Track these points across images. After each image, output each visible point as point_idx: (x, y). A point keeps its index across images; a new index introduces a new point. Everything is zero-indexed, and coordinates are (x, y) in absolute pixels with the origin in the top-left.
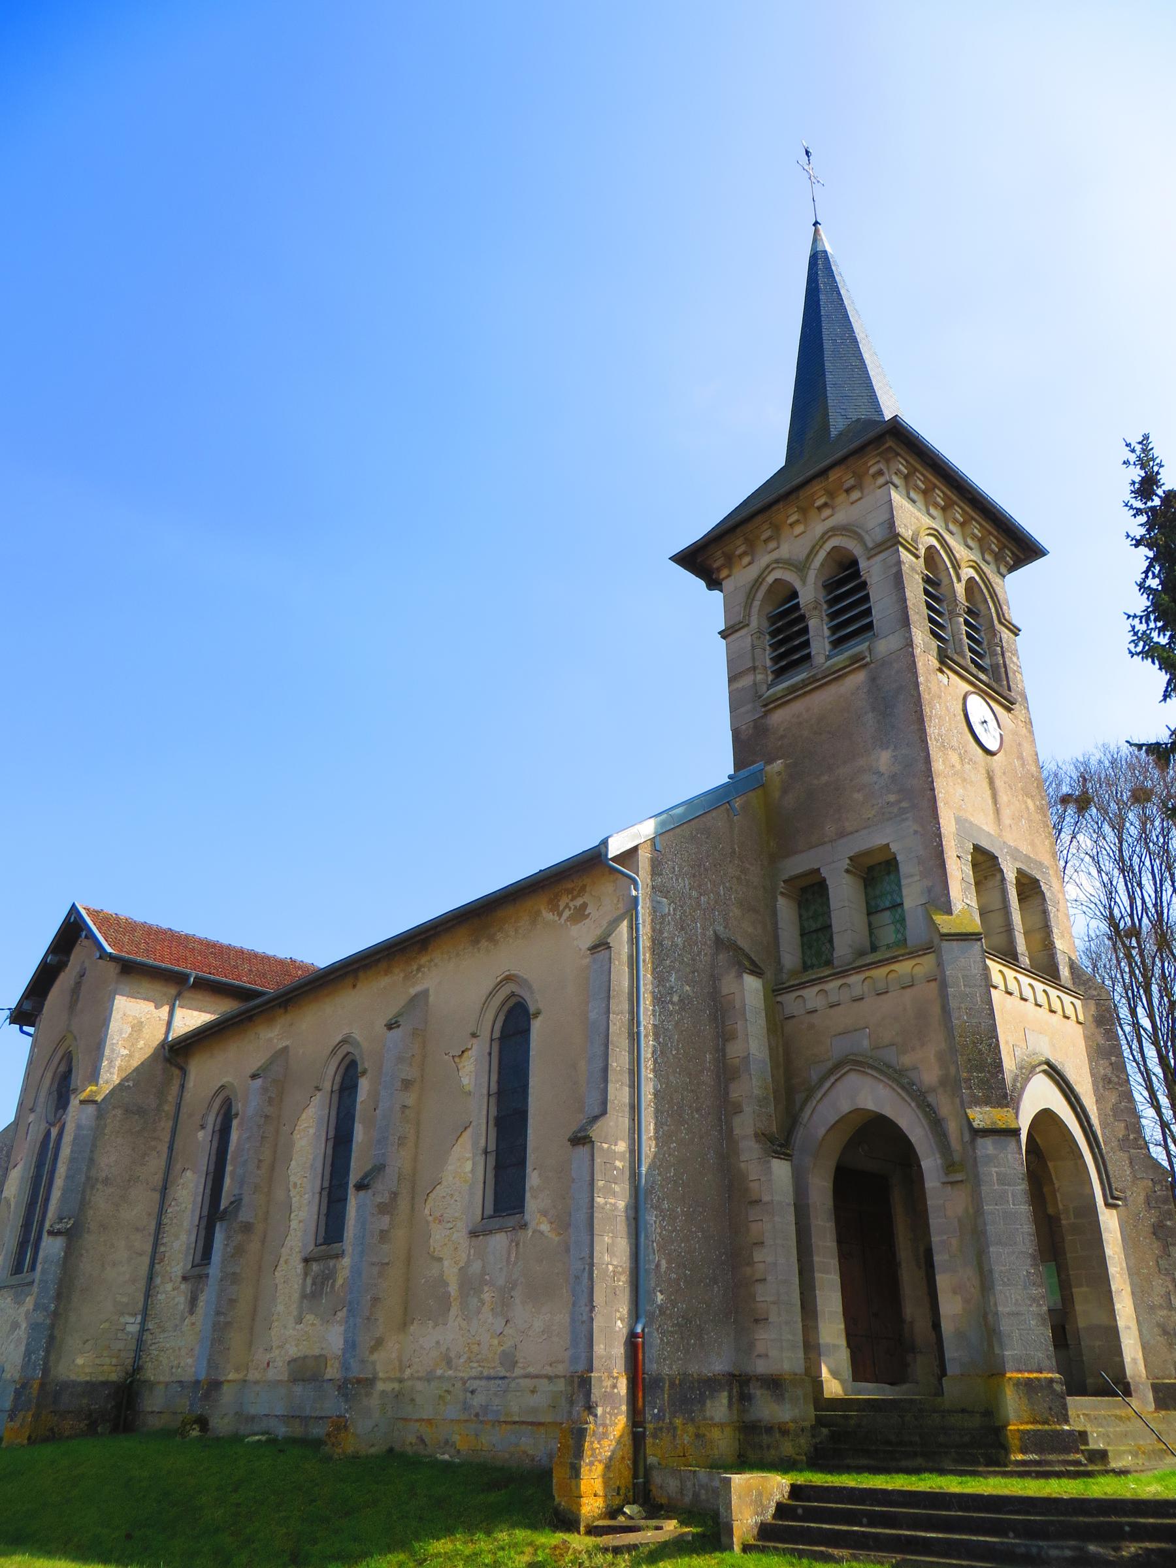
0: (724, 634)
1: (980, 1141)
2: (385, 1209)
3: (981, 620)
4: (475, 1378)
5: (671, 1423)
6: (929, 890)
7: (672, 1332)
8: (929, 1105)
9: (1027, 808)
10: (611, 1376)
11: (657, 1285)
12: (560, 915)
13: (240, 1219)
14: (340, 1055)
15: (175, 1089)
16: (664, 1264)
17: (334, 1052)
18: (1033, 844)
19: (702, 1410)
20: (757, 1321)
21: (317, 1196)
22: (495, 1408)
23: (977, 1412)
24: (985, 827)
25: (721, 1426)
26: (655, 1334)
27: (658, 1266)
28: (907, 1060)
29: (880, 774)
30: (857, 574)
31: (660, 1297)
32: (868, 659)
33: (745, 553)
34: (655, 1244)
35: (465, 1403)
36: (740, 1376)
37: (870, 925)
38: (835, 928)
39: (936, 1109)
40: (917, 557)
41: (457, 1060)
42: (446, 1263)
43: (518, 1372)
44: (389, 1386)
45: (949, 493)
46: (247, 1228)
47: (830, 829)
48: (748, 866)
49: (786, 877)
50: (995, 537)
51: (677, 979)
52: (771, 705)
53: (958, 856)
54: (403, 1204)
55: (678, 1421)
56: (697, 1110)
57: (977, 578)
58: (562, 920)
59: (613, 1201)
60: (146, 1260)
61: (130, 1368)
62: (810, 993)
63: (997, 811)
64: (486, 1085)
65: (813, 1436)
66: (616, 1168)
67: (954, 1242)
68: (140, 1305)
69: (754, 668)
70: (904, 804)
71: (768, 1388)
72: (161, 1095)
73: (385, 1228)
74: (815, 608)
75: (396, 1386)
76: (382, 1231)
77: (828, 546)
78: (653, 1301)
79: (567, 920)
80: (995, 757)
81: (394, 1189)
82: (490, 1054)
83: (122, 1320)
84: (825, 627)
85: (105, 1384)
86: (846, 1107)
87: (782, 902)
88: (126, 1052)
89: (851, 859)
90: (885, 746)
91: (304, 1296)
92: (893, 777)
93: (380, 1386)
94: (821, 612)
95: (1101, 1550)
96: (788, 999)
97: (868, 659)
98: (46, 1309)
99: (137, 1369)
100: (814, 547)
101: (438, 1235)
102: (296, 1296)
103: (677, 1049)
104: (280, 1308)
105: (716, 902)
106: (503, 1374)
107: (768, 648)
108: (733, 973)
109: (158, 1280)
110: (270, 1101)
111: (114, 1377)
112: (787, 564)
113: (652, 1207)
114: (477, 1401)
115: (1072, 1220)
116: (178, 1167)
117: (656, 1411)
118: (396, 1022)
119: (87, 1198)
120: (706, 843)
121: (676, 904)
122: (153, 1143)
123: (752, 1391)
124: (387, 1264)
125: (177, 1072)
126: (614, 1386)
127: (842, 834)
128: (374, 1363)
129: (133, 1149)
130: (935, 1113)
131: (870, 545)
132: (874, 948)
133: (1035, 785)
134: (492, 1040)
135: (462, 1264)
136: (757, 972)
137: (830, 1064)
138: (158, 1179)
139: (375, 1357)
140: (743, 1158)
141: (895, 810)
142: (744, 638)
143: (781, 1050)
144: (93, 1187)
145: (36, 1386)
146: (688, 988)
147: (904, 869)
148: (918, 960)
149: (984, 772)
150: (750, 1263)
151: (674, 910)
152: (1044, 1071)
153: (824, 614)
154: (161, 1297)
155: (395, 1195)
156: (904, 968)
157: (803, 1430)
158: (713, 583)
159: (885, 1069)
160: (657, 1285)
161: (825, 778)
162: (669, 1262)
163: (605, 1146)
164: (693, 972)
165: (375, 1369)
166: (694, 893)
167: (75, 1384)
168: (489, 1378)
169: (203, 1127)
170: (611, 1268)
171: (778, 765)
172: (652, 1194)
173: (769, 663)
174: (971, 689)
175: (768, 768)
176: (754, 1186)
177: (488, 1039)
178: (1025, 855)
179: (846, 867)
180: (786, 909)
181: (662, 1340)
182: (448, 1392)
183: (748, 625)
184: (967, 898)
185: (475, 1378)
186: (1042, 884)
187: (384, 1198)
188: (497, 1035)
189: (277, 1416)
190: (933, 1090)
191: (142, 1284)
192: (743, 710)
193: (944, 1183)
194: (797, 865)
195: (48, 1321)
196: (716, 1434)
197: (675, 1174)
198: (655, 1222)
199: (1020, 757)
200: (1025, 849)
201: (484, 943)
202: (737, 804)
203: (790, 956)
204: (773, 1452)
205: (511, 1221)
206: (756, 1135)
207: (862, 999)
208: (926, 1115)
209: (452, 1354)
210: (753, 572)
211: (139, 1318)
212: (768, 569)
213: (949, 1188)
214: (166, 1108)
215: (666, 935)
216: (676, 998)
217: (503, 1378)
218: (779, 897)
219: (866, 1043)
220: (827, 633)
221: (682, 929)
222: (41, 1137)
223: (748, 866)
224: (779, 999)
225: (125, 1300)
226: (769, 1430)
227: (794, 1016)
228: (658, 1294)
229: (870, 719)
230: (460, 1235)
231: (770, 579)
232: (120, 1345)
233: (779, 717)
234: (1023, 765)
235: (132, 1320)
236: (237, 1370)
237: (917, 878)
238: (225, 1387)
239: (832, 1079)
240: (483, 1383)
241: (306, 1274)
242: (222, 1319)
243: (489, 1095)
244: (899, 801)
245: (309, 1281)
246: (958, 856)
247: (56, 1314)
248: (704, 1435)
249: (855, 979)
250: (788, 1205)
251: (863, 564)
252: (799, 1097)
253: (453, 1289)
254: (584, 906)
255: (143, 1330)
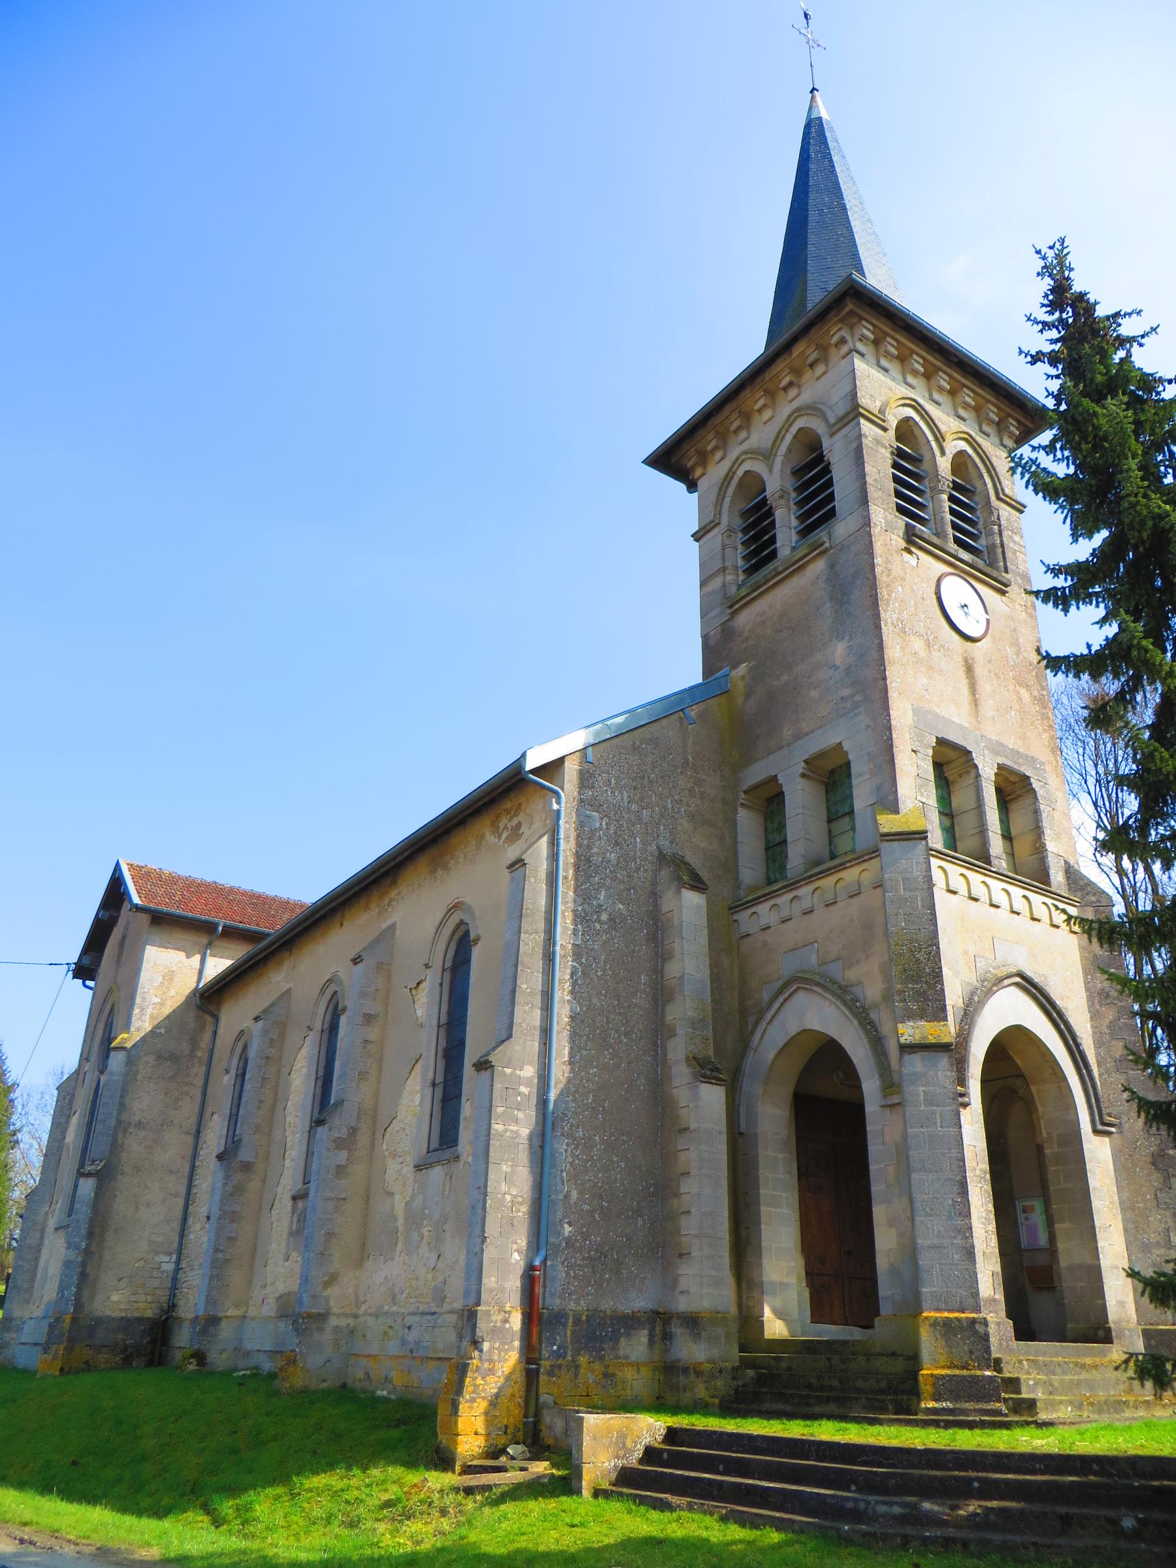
0: (697, 537)
1: (907, 1057)
2: (340, 1144)
3: (977, 498)
4: (413, 1314)
5: (573, 1360)
6: (879, 789)
7: (580, 1265)
8: (871, 1023)
9: (1020, 699)
10: (501, 1310)
11: (565, 1217)
12: (500, 837)
13: (240, 1158)
14: (329, 993)
15: (207, 1036)
16: (574, 1195)
17: (323, 991)
18: (1024, 738)
19: (614, 1348)
20: (681, 1255)
21: (306, 1134)
22: (425, 1344)
23: (902, 1355)
24: (955, 719)
25: (637, 1366)
26: (560, 1267)
27: (567, 1196)
28: (852, 975)
29: (835, 667)
30: (820, 458)
31: (567, 1229)
32: (827, 545)
33: (716, 448)
34: (564, 1174)
35: (403, 1339)
36: (664, 1314)
37: (830, 832)
38: (789, 839)
39: (878, 1026)
40: (885, 430)
41: (414, 992)
42: (397, 1197)
43: (446, 1307)
44: (343, 1322)
45: (929, 358)
46: (247, 1167)
47: (787, 732)
48: (703, 777)
49: (745, 787)
50: (995, 406)
51: (608, 897)
52: (736, 605)
53: (913, 751)
54: (363, 1139)
55: (583, 1360)
56: (626, 1034)
57: (970, 451)
58: (501, 842)
59: (515, 1128)
60: (181, 1202)
61: (165, 1306)
62: (763, 908)
63: (975, 703)
64: (436, 1016)
65: (734, 1378)
66: (519, 1094)
67: (891, 1170)
68: (175, 1245)
69: (724, 570)
70: (857, 698)
71: (687, 1327)
72: (194, 1042)
73: (343, 1163)
74: (782, 497)
75: (351, 1321)
76: (338, 1166)
77: (794, 430)
78: (559, 1233)
79: (504, 842)
80: (978, 644)
81: (353, 1124)
82: (441, 984)
83: (157, 1259)
84: (793, 517)
85: (140, 1320)
86: (793, 1030)
87: (742, 814)
88: (157, 1000)
89: (806, 762)
90: (839, 636)
91: (291, 1234)
92: (848, 671)
93: (333, 1321)
94: (788, 501)
95: (936, 1508)
96: (743, 916)
97: (827, 545)
98: (77, 1247)
99: (172, 1307)
100: (780, 432)
101: (392, 1167)
102: (285, 1233)
103: (604, 971)
104: (274, 1246)
105: (662, 816)
106: (433, 1310)
107: (740, 546)
108: (673, 890)
109: (190, 1221)
110: (272, 1042)
111: (149, 1314)
112: (755, 453)
113: (562, 1135)
114: (412, 1337)
115: (1056, 1149)
116: (208, 1111)
117: (555, 1348)
118: (359, 957)
119: (120, 1141)
120: (652, 753)
121: (610, 818)
122: (186, 1089)
123: (673, 1330)
124: (344, 1199)
125: (209, 1019)
126: (506, 1321)
127: (798, 737)
128: (327, 1299)
129: (166, 1094)
130: (876, 1030)
131: (832, 420)
132: (833, 857)
133: (1034, 673)
134: (444, 970)
135: (408, 1199)
136: (698, 884)
137: (780, 983)
138: (192, 1122)
139: (327, 1292)
140: (675, 1084)
141: (849, 705)
142: (715, 538)
143: (736, 970)
144: (125, 1131)
145: (68, 1319)
146: (621, 906)
147: (855, 769)
148: (865, 866)
149: (961, 659)
150: (677, 1195)
151: (607, 824)
152: (1016, 984)
153: (792, 503)
154: (192, 1236)
155: (354, 1131)
156: (850, 875)
157: (721, 1371)
158: (692, 486)
159: (829, 985)
160: (565, 1217)
161: (785, 678)
162: (581, 1193)
163: (508, 1071)
164: (629, 890)
165: (328, 1304)
166: (634, 807)
167: (110, 1320)
168: (423, 1314)
169: (227, 1071)
170: (508, 1198)
171: (742, 669)
172: (563, 1121)
173: (740, 562)
174: (950, 570)
175: (733, 673)
176: (683, 1112)
177: (440, 969)
178: (1012, 750)
179: (801, 771)
180: (748, 822)
181: (567, 1273)
182: (390, 1327)
183: (718, 524)
184: (922, 795)
185: (413, 1314)
186: (1032, 781)
187: (343, 1133)
188: (449, 964)
189: (265, 1351)
190: (876, 1006)
191: (176, 1225)
192: (712, 614)
193: (882, 1106)
194: (756, 774)
195: (80, 1259)
196: (629, 1374)
197: (594, 1101)
198: (566, 1151)
199: (1016, 644)
200: (1011, 742)
201: (440, 872)
202: (693, 712)
203: (751, 871)
204: (688, 1394)
205: (447, 1154)
206: (687, 1059)
207: (812, 911)
208: (867, 1033)
209: (397, 1290)
210: (726, 464)
211: (174, 1257)
212: (738, 462)
213: (888, 1110)
214: (199, 1054)
215: (595, 850)
216: (604, 917)
217: (433, 1314)
218: (740, 810)
219: (814, 959)
220: (794, 522)
221: (617, 844)
222: (94, 1086)
223: (703, 777)
224: (735, 917)
225: (159, 1239)
226: (686, 1370)
227: (749, 935)
228: (566, 1226)
229: (828, 609)
230: (408, 1170)
231: (740, 473)
232: (156, 1283)
233: (745, 618)
234: (1018, 653)
235: (167, 1259)
236: (237, 1306)
237: (868, 776)
238: (224, 1324)
239: (781, 999)
240: (416, 1318)
241: (293, 1212)
242: (220, 1256)
243: (439, 1026)
244: (853, 695)
245: (295, 1219)
246: (913, 751)
247: (87, 1252)
248: (614, 1375)
249: (805, 891)
250: (720, 1133)
251: (826, 443)
252: (751, 1020)
253: (400, 1222)
254: (519, 825)
255: (178, 1269)
